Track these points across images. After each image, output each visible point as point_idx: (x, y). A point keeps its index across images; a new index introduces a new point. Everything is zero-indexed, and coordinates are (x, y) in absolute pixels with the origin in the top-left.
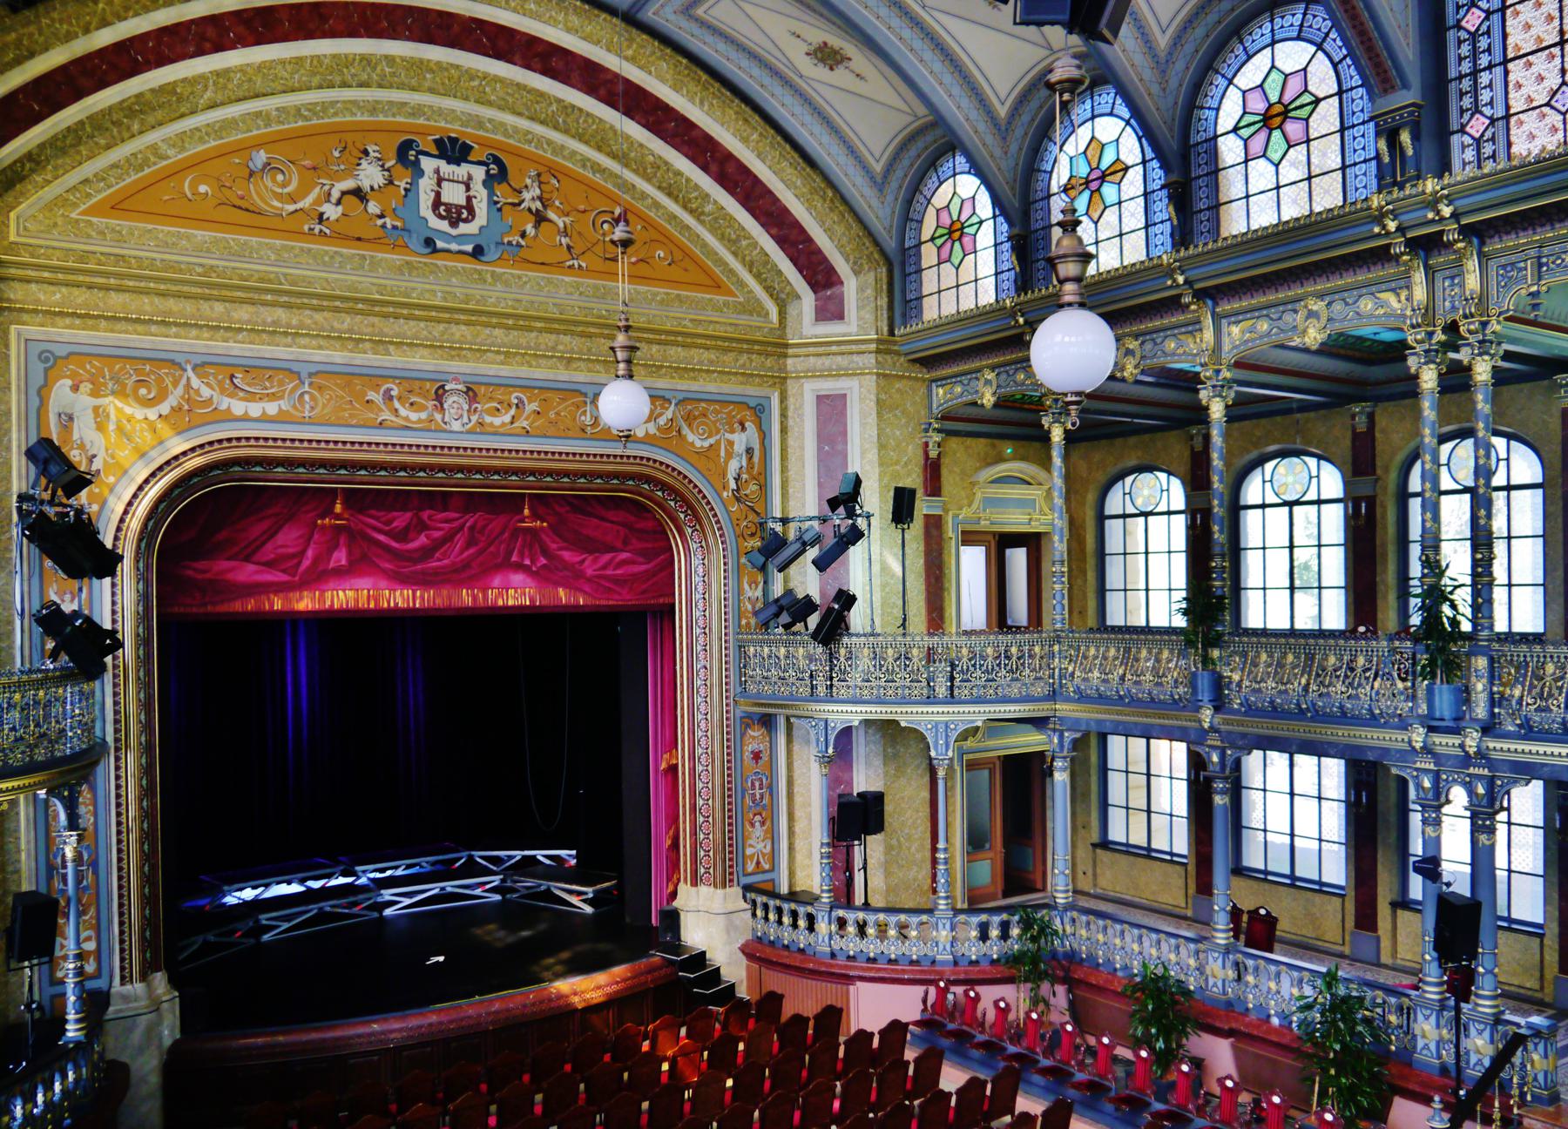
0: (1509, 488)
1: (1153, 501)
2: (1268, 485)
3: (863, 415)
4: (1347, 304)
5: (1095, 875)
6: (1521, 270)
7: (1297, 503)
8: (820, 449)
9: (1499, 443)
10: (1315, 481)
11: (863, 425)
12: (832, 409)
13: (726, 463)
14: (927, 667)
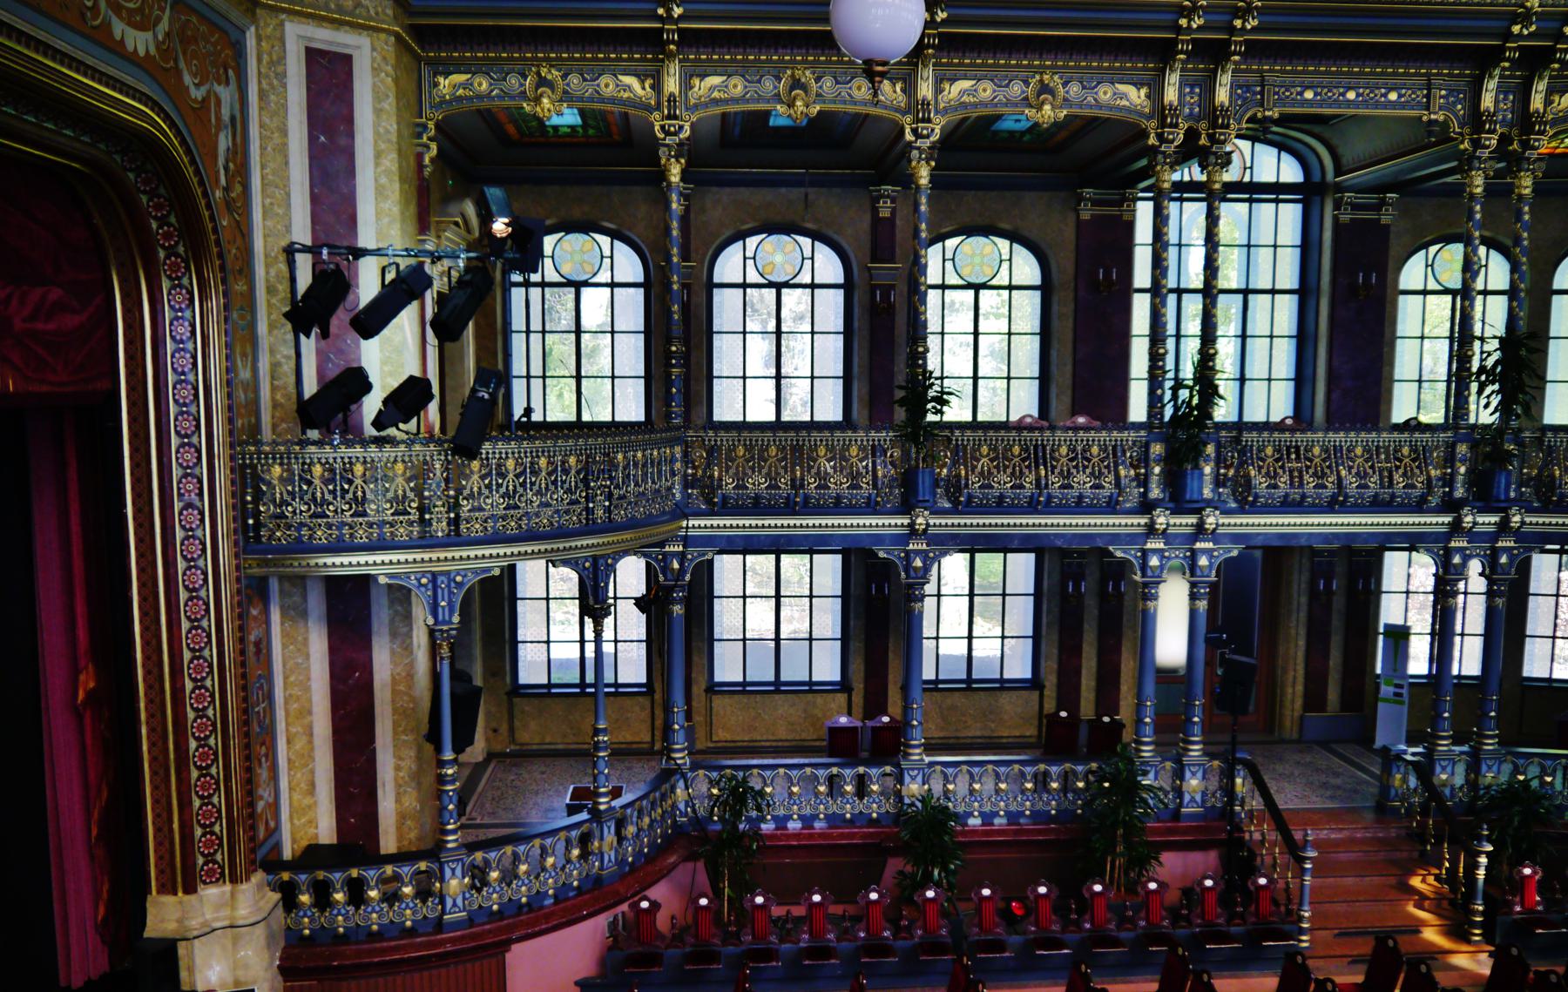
0: (1485, 293)
1: (588, 268)
2: (750, 263)
3: (378, 97)
4: (1084, 88)
5: (512, 730)
6: (1255, 93)
7: (787, 285)
8: (312, 139)
9: (1482, 250)
10: (808, 263)
11: (378, 112)
12: (329, 77)
13: (217, 135)
14: (586, 481)
